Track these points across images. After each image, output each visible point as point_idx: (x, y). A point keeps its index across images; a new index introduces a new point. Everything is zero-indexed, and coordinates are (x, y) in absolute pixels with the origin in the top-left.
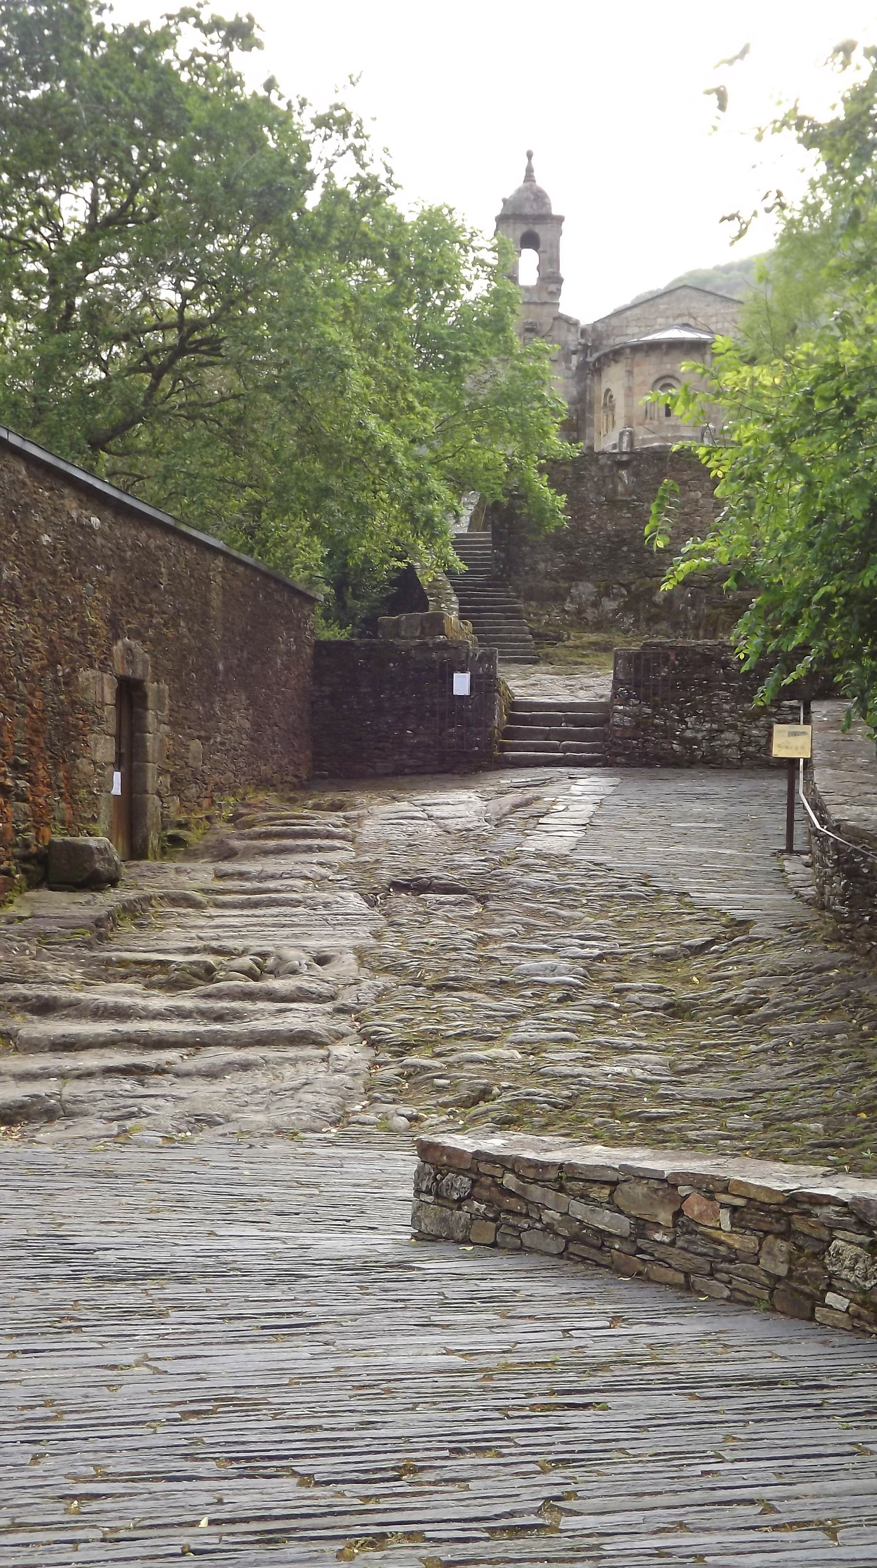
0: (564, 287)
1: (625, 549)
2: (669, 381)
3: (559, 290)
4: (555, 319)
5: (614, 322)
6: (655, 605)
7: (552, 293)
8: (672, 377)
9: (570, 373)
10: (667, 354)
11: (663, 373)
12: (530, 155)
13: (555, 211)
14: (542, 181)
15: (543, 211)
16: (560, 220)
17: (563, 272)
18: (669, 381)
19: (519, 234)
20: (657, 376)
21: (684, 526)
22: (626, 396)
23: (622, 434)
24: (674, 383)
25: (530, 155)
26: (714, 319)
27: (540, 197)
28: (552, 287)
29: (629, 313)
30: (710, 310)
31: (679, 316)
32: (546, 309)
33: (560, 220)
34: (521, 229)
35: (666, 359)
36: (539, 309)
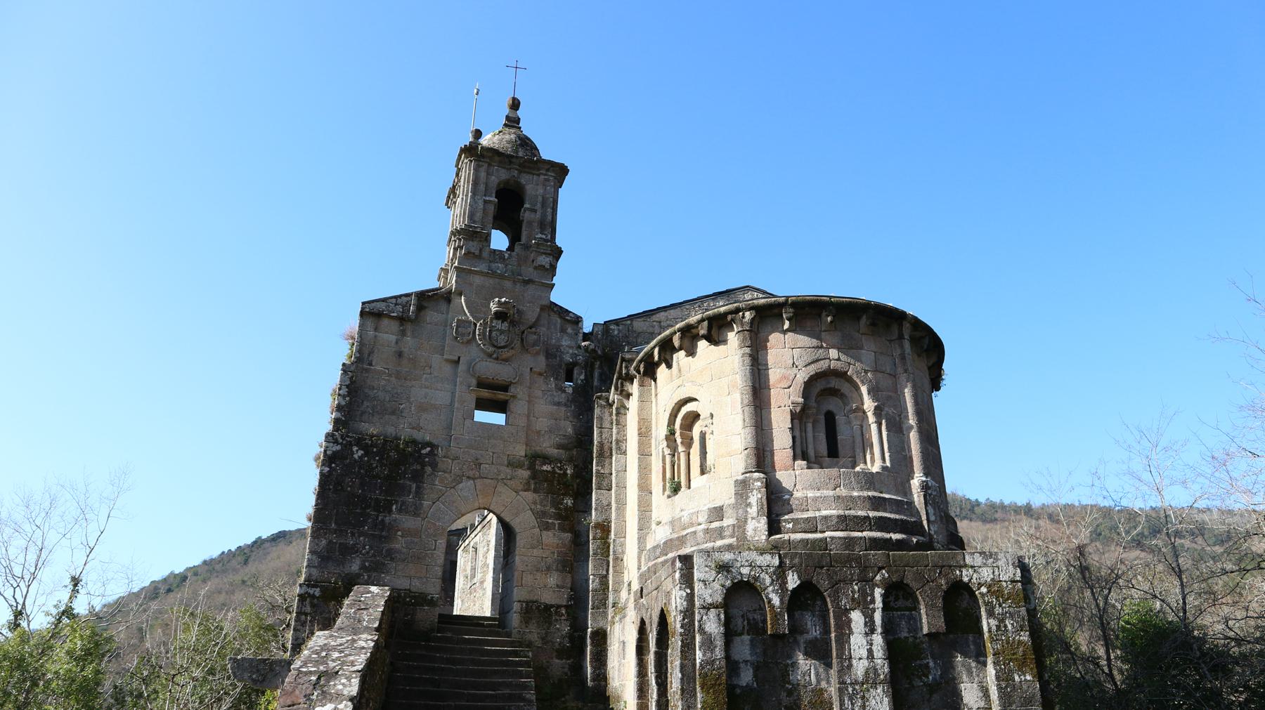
2: (834, 383)
3: (552, 270)
4: (543, 308)
5: (639, 325)
9: (562, 398)
12: (515, 105)
16: (560, 171)
18: (834, 383)
19: (494, 180)
20: (812, 369)
25: (515, 105)
28: (544, 260)
29: (662, 315)
32: (531, 290)
33: (560, 171)
34: (500, 175)
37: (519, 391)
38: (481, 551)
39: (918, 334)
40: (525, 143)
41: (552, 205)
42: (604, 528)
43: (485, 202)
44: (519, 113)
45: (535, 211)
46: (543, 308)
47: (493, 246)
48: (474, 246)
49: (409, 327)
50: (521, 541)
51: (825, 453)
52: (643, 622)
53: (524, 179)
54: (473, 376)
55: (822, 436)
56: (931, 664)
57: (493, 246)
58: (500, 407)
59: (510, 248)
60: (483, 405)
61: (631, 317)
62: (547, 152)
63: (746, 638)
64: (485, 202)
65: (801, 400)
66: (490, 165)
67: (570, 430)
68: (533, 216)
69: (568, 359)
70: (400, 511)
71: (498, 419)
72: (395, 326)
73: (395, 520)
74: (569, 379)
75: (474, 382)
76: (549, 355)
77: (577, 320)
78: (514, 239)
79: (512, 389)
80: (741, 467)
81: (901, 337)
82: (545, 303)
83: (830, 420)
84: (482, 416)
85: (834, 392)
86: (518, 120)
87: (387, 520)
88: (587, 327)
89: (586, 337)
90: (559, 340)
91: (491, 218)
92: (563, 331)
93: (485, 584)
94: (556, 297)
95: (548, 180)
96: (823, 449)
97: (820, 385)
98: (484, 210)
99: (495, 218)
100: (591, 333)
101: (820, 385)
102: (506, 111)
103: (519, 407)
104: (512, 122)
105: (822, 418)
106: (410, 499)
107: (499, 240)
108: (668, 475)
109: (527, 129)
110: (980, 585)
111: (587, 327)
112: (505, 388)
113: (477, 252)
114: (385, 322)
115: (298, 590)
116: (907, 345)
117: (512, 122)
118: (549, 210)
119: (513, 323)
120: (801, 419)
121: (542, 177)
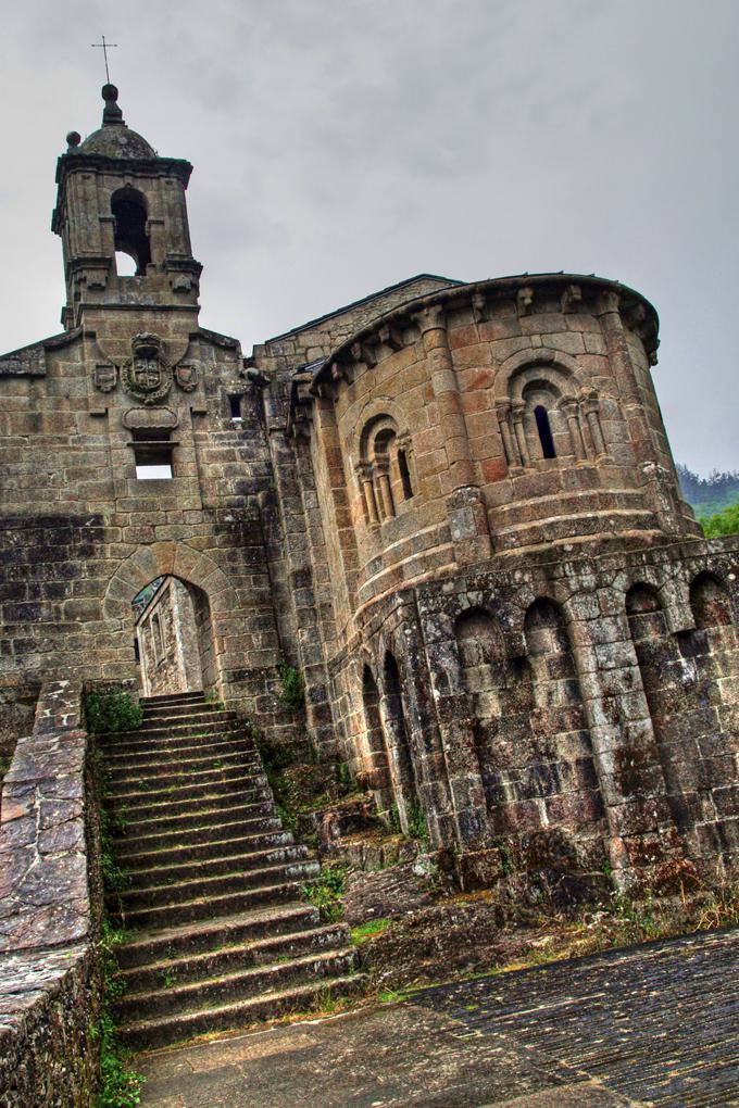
0: (203, 282)
2: (542, 374)
3: (194, 288)
4: (192, 337)
7: (180, 291)
8: (548, 364)
10: (529, 311)
11: (533, 355)
12: (110, 93)
16: (182, 170)
17: (197, 256)
18: (542, 374)
19: (108, 192)
20: (515, 363)
24: (552, 377)
25: (110, 93)
28: (182, 280)
29: (330, 325)
32: (175, 320)
33: (182, 170)
34: (112, 185)
36: (160, 319)
37: (183, 437)
38: (165, 622)
39: (627, 304)
40: (135, 141)
41: (180, 211)
42: (304, 576)
43: (101, 220)
45: (162, 223)
46: (192, 337)
47: (121, 273)
48: (94, 276)
49: (41, 387)
50: (214, 605)
51: (541, 455)
52: (367, 669)
53: (140, 186)
54: (127, 429)
55: (535, 435)
56: (684, 664)
57: (121, 273)
58: (164, 456)
59: (141, 272)
60: (144, 458)
61: (296, 332)
62: (164, 149)
63: (484, 666)
64: (101, 220)
65: (506, 398)
66: (97, 174)
67: (249, 471)
68: (160, 229)
69: (230, 390)
70: (76, 593)
71: (162, 472)
72: (24, 386)
73: (70, 605)
74: (236, 413)
75: (130, 440)
76: (210, 390)
77: (232, 347)
78: (143, 261)
79: (174, 438)
82: (195, 331)
83: (541, 414)
84: (146, 472)
86: (119, 113)
87: (62, 606)
88: (247, 352)
89: (249, 362)
90: (217, 371)
91: (111, 239)
93: (176, 659)
94: (205, 321)
95: (168, 183)
96: (537, 450)
97: (523, 381)
98: (102, 230)
99: (117, 237)
100: (253, 358)
101: (523, 381)
102: (103, 104)
103: (185, 455)
104: (113, 116)
105: (531, 415)
106: (85, 577)
107: (126, 265)
108: (369, 505)
109: (134, 121)
110: (729, 572)
111: (247, 352)
112: (166, 433)
113: (104, 284)
114: (13, 383)
115: (539, 681)
116: (617, 319)
117: (113, 116)
118: (179, 219)
119: (162, 363)
120: (509, 422)
121: (163, 180)
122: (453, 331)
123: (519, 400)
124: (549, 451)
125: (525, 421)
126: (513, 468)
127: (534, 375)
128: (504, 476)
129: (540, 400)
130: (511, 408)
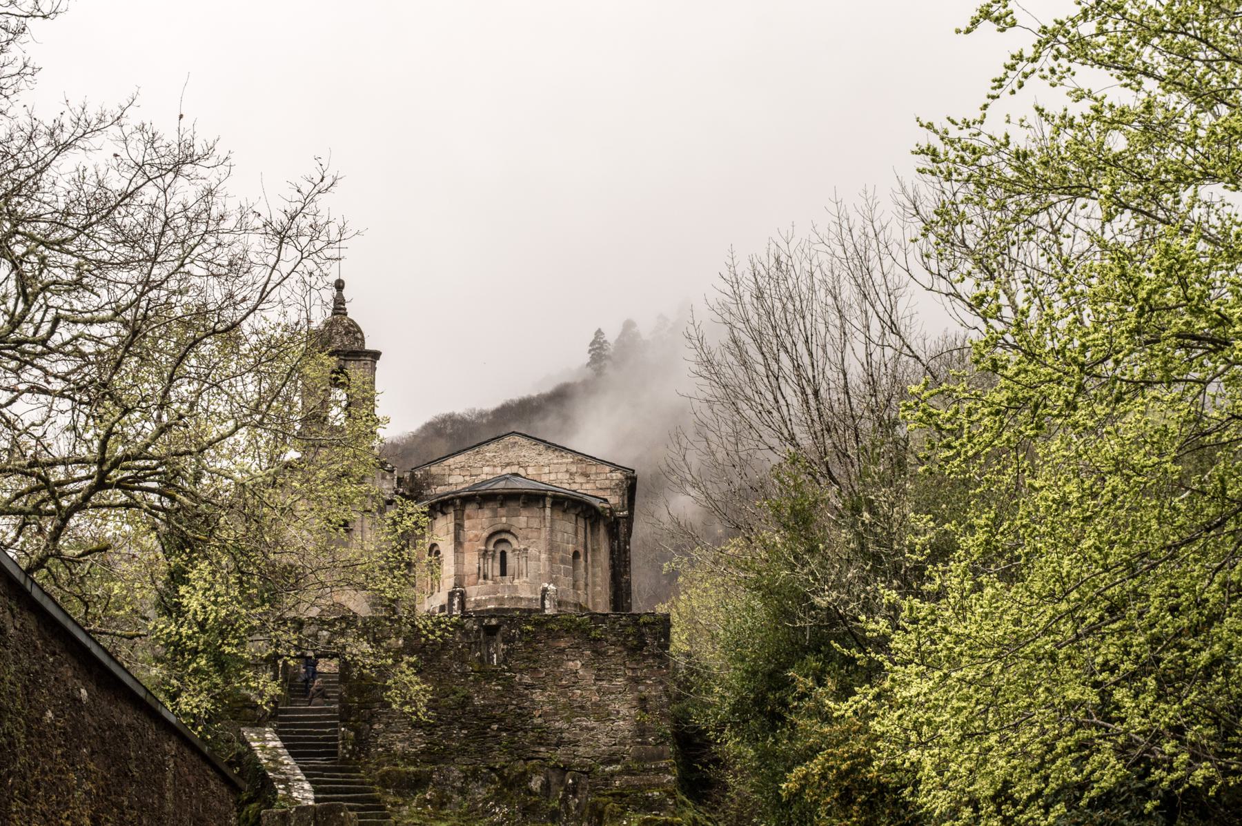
1: (495, 727)
2: (504, 536)
6: (530, 792)
8: (509, 532)
11: (499, 527)
12: (339, 285)
13: (368, 347)
14: (354, 312)
15: (356, 346)
16: (376, 355)
18: (504, 536)
20: (491, 530)
21: (562, 700)
22: (456, 550)
23: (451, 595)
24: (509, 537)
26: (546, 470)
27: (353, 331)
30: (543, 460)
31: (508, 464)
33: (376, 355)
35: (502, 511)
44: (345, 292)
55: (497, 565)
80: (452, 585)
81: (544, 507)
83: (503, 554)
85: (505, 541)
92: (383, 478)
96: (497, 572)
104: (339, 306)
105: (498, 555)
116: (548, 511)
117: (339, 306)
122: (467, 511)
123: (491, 548)
124: (503, 573)
125: (493, 557)
126: (481, 580)
127: (499, 537)
128: (476, 584)
129: (502, 547)
130: (486, 551)
